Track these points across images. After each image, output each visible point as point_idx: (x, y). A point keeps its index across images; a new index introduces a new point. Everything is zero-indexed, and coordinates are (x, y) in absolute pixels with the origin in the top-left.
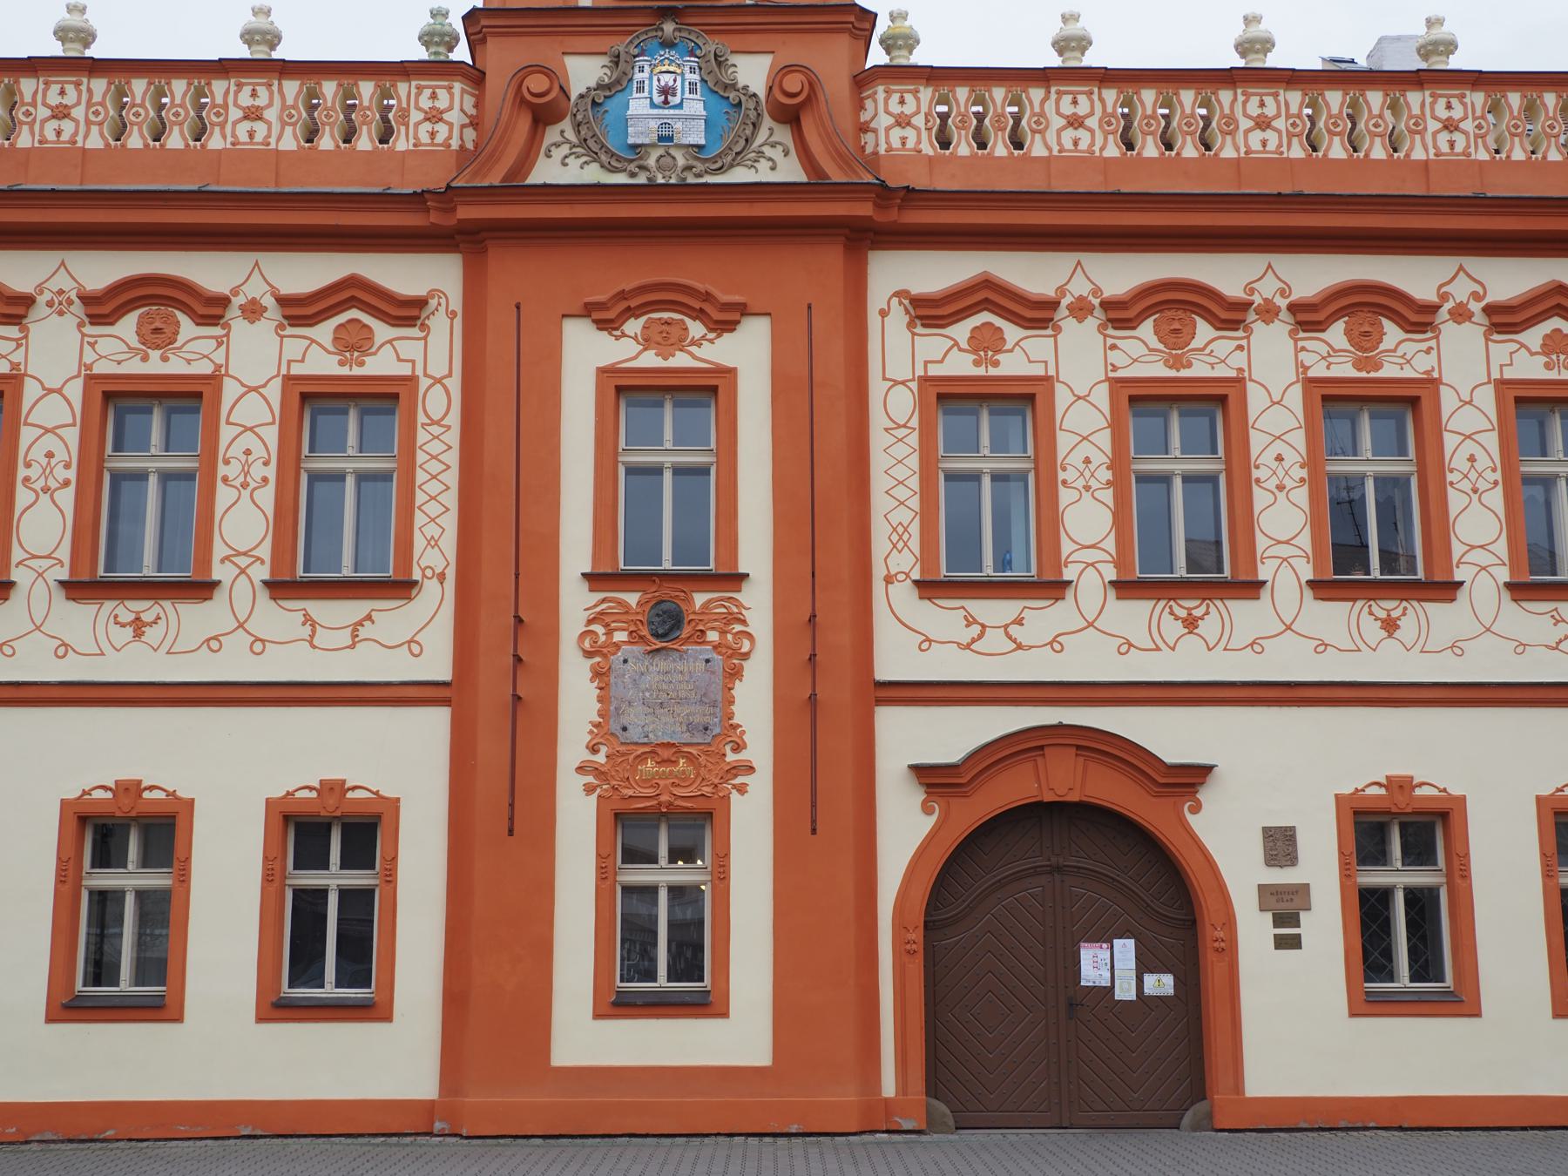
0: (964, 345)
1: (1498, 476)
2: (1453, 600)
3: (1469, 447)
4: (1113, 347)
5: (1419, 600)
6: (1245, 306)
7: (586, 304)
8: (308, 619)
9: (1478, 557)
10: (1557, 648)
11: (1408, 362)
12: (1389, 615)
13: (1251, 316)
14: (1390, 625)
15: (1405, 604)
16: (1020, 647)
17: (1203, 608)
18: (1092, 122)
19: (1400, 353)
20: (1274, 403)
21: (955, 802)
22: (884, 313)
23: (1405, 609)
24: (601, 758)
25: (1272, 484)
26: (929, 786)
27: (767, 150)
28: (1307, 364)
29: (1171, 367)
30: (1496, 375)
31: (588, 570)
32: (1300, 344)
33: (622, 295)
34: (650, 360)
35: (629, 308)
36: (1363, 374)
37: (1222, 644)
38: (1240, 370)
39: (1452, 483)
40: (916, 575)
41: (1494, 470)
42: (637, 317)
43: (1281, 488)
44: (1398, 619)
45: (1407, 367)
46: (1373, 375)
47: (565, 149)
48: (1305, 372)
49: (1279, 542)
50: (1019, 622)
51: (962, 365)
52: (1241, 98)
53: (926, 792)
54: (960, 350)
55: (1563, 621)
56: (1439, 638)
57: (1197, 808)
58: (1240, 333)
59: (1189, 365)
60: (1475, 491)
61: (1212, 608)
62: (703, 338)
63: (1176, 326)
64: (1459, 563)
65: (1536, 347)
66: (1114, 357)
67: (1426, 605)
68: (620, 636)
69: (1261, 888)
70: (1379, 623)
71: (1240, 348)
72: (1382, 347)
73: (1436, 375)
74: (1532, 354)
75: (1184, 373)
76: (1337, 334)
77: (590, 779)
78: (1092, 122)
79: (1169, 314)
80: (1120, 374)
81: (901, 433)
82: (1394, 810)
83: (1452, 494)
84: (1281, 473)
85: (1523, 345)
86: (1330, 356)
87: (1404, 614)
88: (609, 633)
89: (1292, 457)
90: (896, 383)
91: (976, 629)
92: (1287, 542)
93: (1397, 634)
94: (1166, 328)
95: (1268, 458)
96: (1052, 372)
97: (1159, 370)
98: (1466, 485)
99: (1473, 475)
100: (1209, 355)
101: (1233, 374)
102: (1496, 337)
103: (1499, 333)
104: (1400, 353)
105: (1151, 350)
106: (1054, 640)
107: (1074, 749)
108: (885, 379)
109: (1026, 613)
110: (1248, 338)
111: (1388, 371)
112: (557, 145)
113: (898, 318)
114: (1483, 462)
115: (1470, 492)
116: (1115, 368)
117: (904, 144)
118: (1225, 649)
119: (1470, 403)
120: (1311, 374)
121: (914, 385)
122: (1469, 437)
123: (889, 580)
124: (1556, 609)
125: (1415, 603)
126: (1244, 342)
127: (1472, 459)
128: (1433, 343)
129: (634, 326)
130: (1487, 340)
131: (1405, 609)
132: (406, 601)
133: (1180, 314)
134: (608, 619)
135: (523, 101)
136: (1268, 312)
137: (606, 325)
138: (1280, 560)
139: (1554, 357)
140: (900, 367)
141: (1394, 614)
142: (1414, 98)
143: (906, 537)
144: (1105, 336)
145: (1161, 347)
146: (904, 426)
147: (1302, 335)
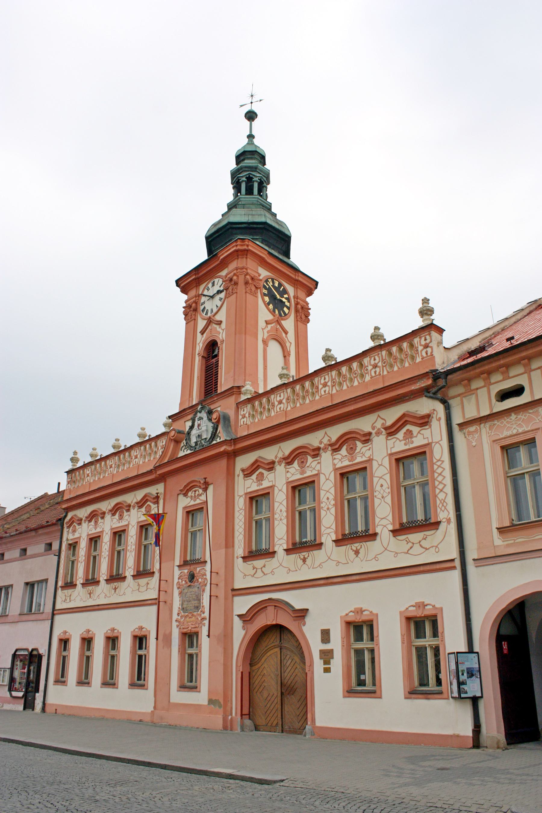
0: (255, 481)
1: (389, 490)
2: (375, 540)
3: (382, 481)
4: (288, 472)
5: (365, 542)
6: (319, 449)
7: (180, 490)
8: (139, 585)
9: (384, 522)
10: (407, 553)
11: (364, 455)
12: (357, 549)
13: (321, 451)
14: (357, 552)
15: (361, 544)
16: (265, 574)
17: (307, 554)
18: (284, 401)
19: (361, 452)
20: (327, 480)
21: (249, 626)
22: (238, 476)
23: (361, 546)
24: (179, 617)
25: (325, 509)
26: (244, 621)
27: (219, 435)
28: (336, 463)
29: (301, 474)
30: (389, 452)
31: (178, 564)
32: (334, 457)
33: (185, 486)
34: (193, 503)
35: (187, 490)
36: (351, 463)
37: (312, 567)
38: (318, 471)
39: (376, 496)
40: (242, 556)
41: (388, 488)
42: (190, 491)
43: (328, 509)
44: (359, 550)
45: (363, 457)
46: (354, 462)
47: (184, 447)
48: (335, 467)
49: (328, 528)
50: (264, 566)
51: (254, 487)
52: (319, 379)
53: (243, 623)
54: (255, 482)
55: (410, 542)
56: (371, 556)
57: (304, 624)
58: (319, 458)
59: (306, 473)
60: (383, 497)
61: (310, 555)
62: (202, 494)
63: (302, 460)
64: (378, 525)
65: (401, 438)
66: (289, 475)
67: (367, 543)
68: (184, 582)
69: (320, 651)
70: (354, 552)
71: (318, 463)
72: (356, 451)
73: (371, 457)
74: (400, 441)
75: (305, 475)
76: (344, 451)
77: (177, 623)
78: (284, 401)
79: (300, 457)
80: (290, 480)
81: (242, 511)
82: (356, 621)
83: (376, 499)
84: (328, 503)
85: (397, 439)
86: (342, 459)
87: (361, 548)
88: (182, 582)
89: (331, 497)
90: (242, 496)
91: (255, 570)
92: (329, 528)
93: (359, 556)
94: (300, 462)
95: (325, 500)
96: (274, 484)
97: (299, 476)
98: (380, 496)
99: (382, 492)
100: (311, 468)
101: (316, 472)
102: (389, 438)
103: (390, 436)
104: (361, 452)
105: (296, 470)
106: (272, 571)
107: (274, 607)
108: (238, 496)
109: (266, 563)
110: (320, 459)
111: (359, 460)
112: (183, 447)
113: (242, 475)
114: (385, 486)
115: (381, 498)
116: (288, 478)
117: (244, 423)
118: (313, 568)
119: (381, 465)
120: (337, 466)
121: (244, 496)
122: (381, 478)
123: (237, 558)
124: (407, 538)
125: (364, 543)
126: (319, 461)
127: (382, 486)
128: (370, 446)
129: (190, 494)
130: (387, 439)
131: (361, 546)
132: (151, 578)
133: (304, 456)
134: (182, 578)
135: (172, 439)
136: (325, 449)
137: (185, 495)
138: (327, 535)
139: (407, 440)
140: (241, 493)
141: (358, 548)
142: (366, 361)
143: (239, 544)
144: (286, 468)
145: (299, 468)
146: (242, 509)
147: (335, 453)
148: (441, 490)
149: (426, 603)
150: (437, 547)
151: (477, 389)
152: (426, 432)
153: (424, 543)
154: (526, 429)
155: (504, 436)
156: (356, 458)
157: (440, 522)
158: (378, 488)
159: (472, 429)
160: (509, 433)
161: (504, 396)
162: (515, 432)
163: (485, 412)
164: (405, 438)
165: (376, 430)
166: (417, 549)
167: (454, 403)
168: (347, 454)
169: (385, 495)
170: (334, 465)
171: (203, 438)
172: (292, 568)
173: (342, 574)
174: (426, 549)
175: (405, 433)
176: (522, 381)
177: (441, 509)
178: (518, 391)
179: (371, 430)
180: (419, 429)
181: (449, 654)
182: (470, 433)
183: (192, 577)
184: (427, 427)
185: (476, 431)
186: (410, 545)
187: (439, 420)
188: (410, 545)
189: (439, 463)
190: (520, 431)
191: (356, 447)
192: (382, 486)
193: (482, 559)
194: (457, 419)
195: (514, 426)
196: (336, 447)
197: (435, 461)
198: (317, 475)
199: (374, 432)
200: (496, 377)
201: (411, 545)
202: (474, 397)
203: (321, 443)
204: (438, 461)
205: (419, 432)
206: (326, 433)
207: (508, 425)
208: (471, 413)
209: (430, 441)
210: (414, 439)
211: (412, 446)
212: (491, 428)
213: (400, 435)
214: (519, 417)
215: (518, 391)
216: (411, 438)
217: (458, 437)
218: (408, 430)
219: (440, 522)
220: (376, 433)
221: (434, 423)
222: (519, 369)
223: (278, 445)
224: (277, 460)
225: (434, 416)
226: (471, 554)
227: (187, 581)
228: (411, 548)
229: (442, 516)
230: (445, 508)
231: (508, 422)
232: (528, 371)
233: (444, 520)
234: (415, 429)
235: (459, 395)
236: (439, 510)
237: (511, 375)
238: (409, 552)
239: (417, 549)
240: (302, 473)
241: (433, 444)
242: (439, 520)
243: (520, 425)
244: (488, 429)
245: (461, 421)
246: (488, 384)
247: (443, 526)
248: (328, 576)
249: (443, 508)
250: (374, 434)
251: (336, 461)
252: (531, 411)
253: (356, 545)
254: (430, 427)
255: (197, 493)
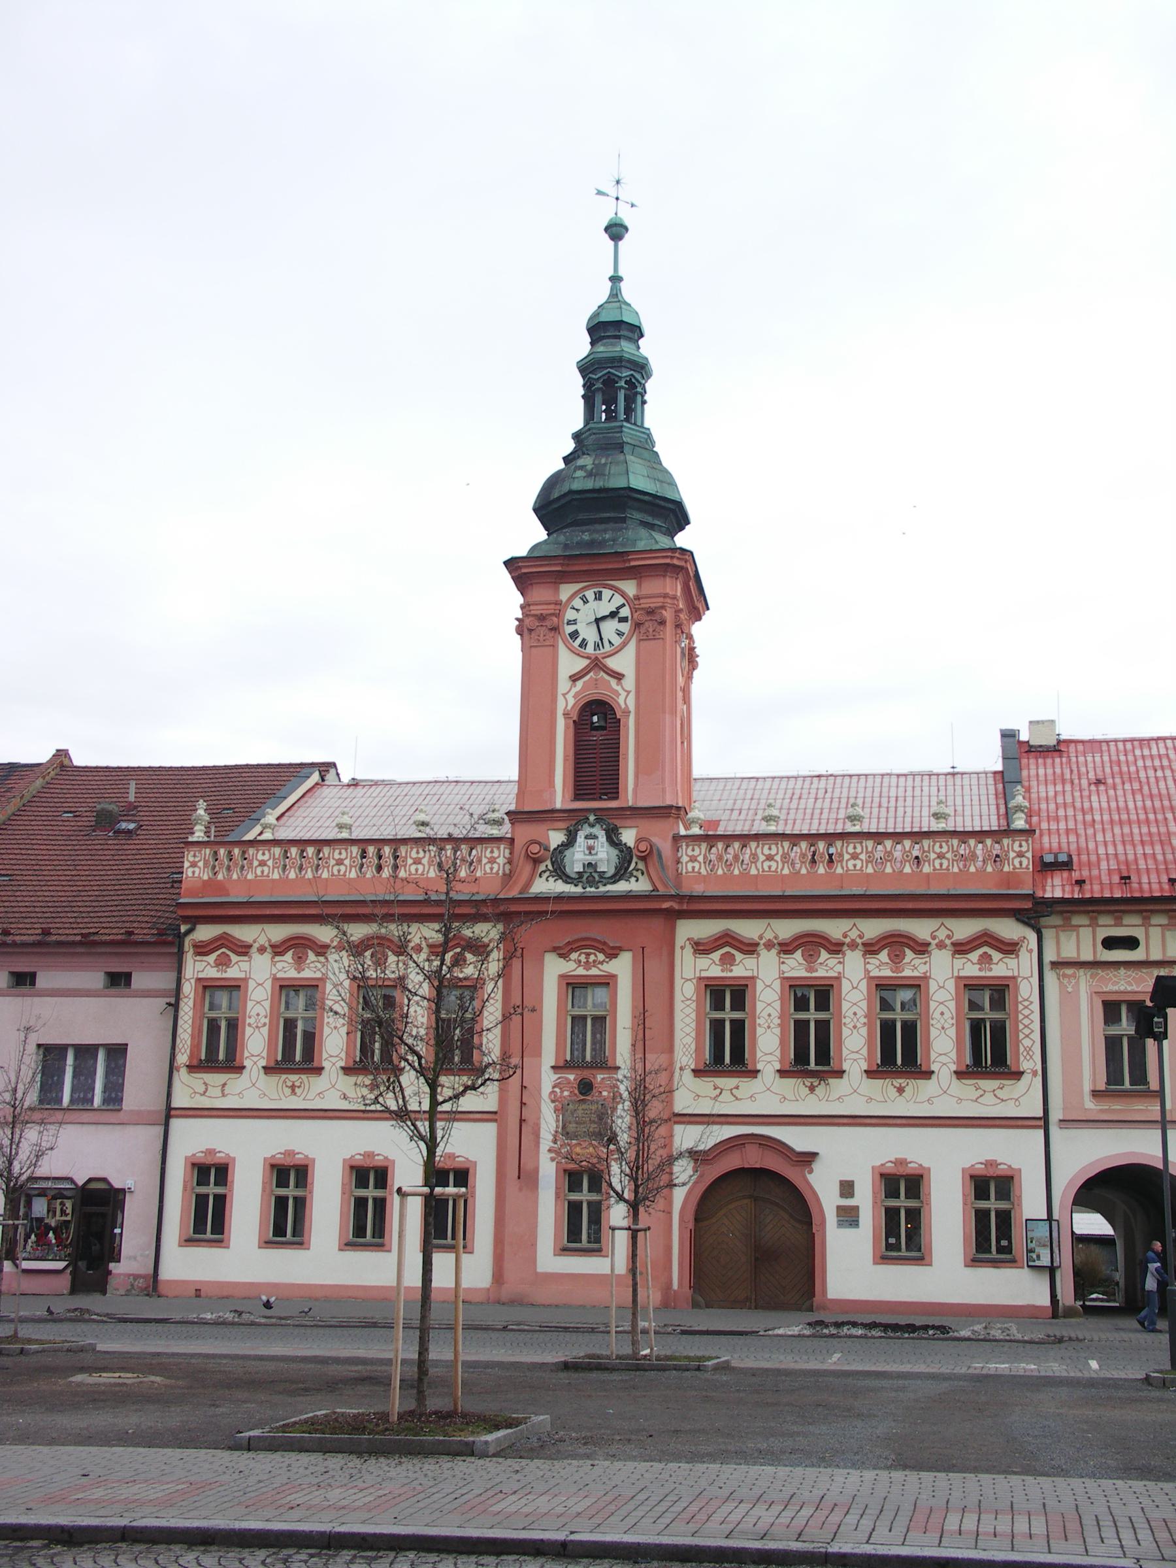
0: (717, 963)
3: (942, 1008)
9: (943, 1059)
13: (845, 948)
14: (901, 1090)
36: (895, 975)
38: (839, 973)
41: (952, 1018)
46: (900, 975)
58: (840, 956)
60: (943, 1028)
65: (975, 961)
66: (783, 967)
72: (904, 961)
75: (814, 975)
80: (786, 975)
95: (850, 1014)
98: (939, 1026)
99: (942, 1021)
111: (907, 973)
114: (947, 1015)
116: (783, 973)
120: (872, 974)
122: (942, 1003)
127: (942, 1014)
128: (928, 959)
148: (1027, 1036)
149: (999, 1161)
150: (1017, 1100)
151: (1080, 926)
152: (1011, 962)
153: (998, 1092)
154: (1136, 989)
155: (1107, 990)
156: (903, 970)
157: (1023, 1073)
158: (937, 1015)
159: (1069, 971)
160: (1115, 988)
161: (1110, 943)
162: (1122, 988)
163: (1087, 956)
164: (980, 962)
165: (937, 941)
166: (989, 1098)
167: (1048, 934)
168: (888, 961)
169: (946, 1026)
170: (867, 971)
171: (598, 870)
172: (790, 1096)
173: (876, 1114)
174: (1002, 1100)
175: (981, 956)
176: (1138, 933)
177: (1025, 1057)
178: (1131, 943)
179: (929, 939)
180: (1002, 956)
181: (1027, 1220)
182: (1065, 976)
183: (586, 1087)
184: (1014, 956)
185: (1074, 975)
186: (980, 1092)
187: (1031, 951)
188: (980, 1092)
189: (1026, 1003)
190: (1129, 989)
191: (904, 955)
192: (942, 1014)
193: (1069, 1121)
194: (1050, 956)
195: (1122, 982)
196: (871, 948)
197: (1020, 999)
198: (838, 979)
199: (934, 942)
200: (1103, 920)
201: (983, 1092)
202: (1075, 933)
203: (845, 936)
204: (1025, 1000)
205: (1001, 960)
206: (855, 925)
207: (1115, 979)
208: (1069, 951)
209: (1016, 974)
210: (992, 966)
211: (989, 974)
212: (1092, 977)
213: (975, 956)
214: (1129, 973)
215: (1131, 943)
216: (990, 964)
217: (1050, 977)
218: (985, 953)
219: (1023, 1073)
220: (936, 945)
221: (1023, 953)
222: (1136, 920)
223: (767, 921)
224: (762, 942)
225: (1025, 945)
226: (1055, 1115)
227: (576, 1092)
228: (981, 1096)
229: (1025, 1065)
230: (1031, 1057)
231: (1115, 976)
232: (1146, 924)
233: (1029, 1071)
234: (996, 955)
235: (1055, 927)
236: (1022, 1058)
237: (1125, 922)
238: (979, 1100)
239: (989, 1098)
240: (810, 970)
241: (1019, 980)
242: (1022, 1070)
243: (1129, 984)
244: (1088, 977)
245: (1054, 959)
246: (1094, 924)
247: (1026, 1079)
248: (853, 1114)
249: (1028, 1057)
250: (933, 946)
251: (869, 967)
252: (1144, 971)
253: (900, 1081)
254: (1017, 956)
255: (592, 958)
